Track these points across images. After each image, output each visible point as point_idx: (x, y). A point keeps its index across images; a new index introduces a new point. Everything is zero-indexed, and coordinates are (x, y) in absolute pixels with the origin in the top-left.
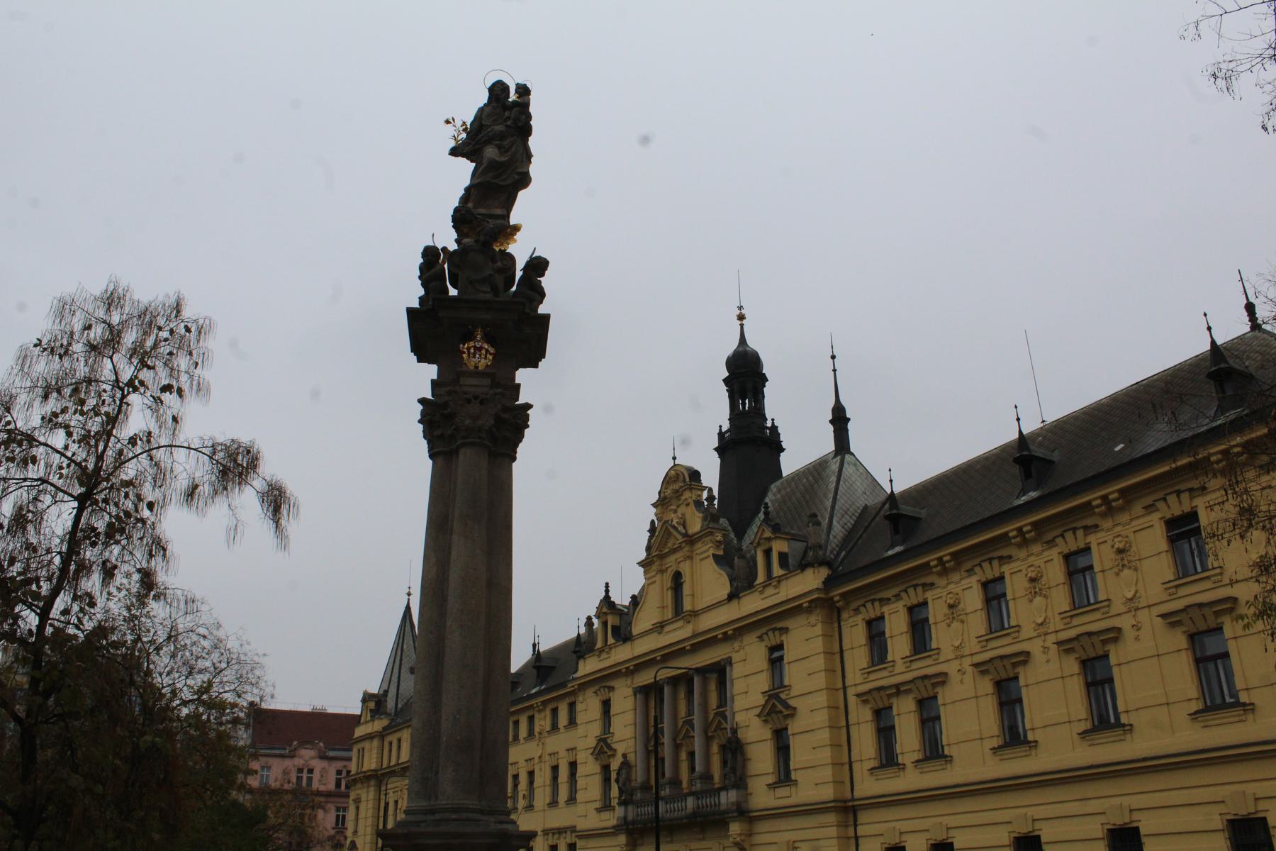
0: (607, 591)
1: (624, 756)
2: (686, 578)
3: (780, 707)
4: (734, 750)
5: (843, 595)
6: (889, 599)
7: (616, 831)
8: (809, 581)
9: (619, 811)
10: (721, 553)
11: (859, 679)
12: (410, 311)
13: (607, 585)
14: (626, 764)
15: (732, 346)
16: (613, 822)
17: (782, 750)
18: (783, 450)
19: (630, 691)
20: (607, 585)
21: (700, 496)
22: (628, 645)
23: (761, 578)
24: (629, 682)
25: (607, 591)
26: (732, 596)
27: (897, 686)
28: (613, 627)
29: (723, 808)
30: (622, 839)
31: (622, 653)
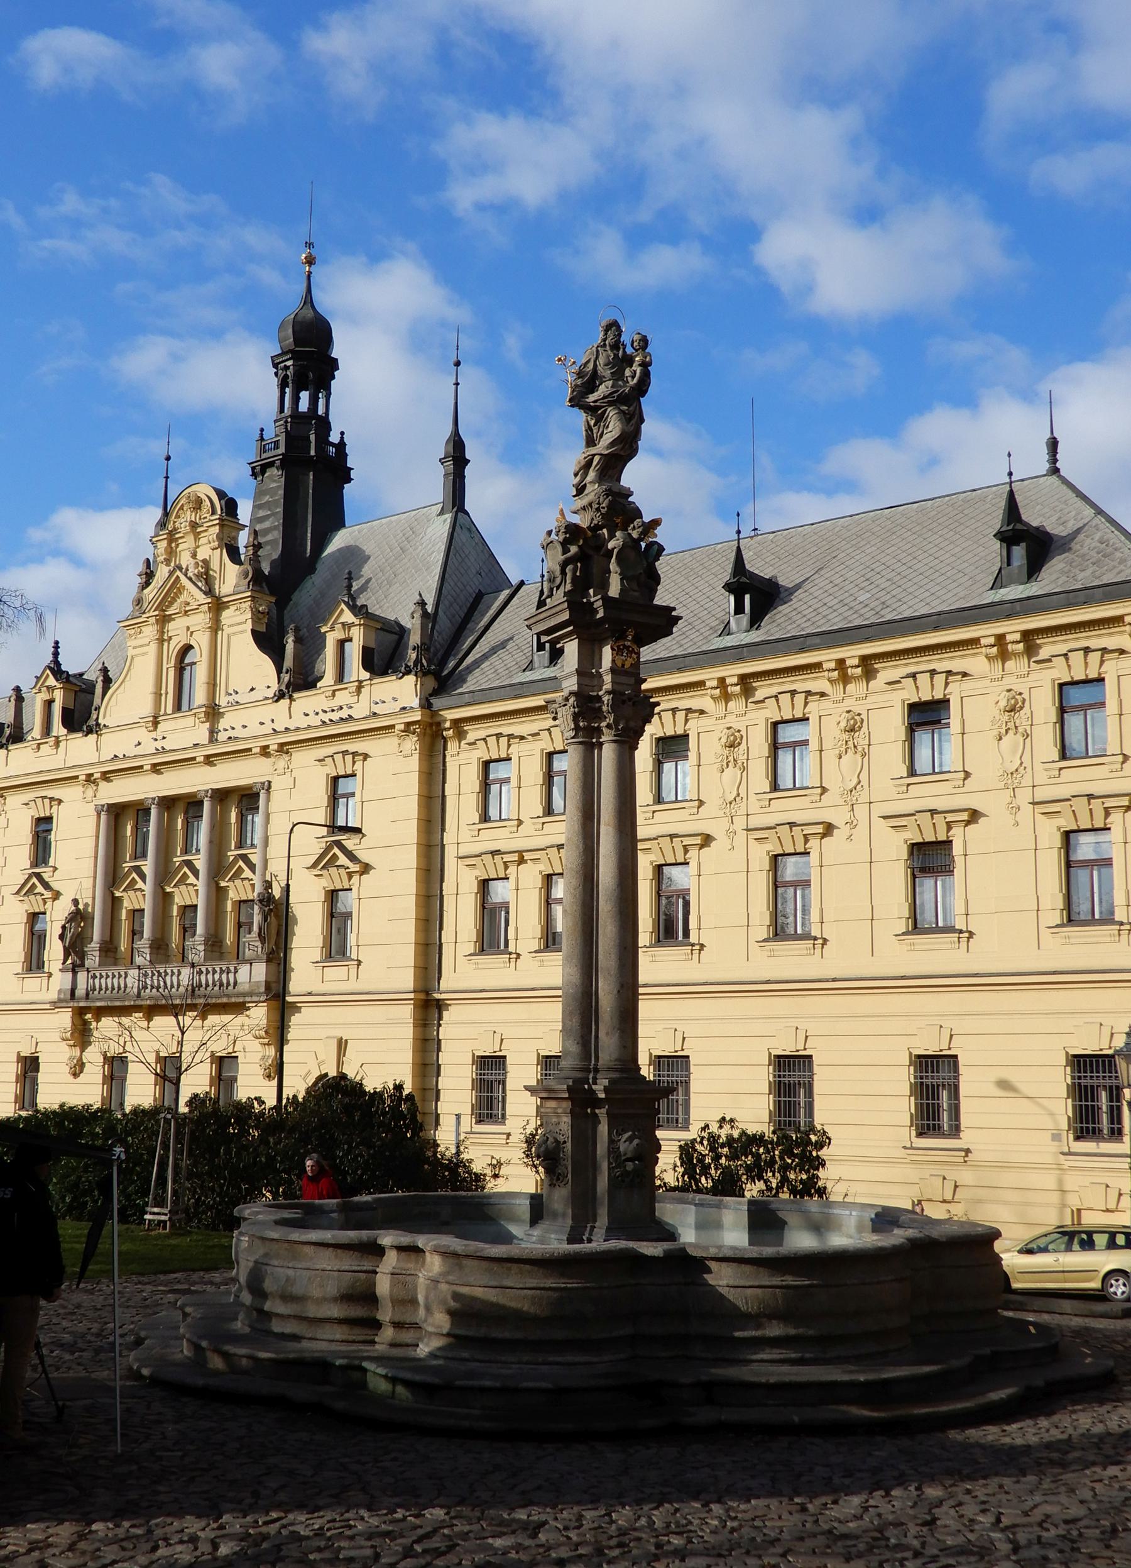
0: (56, 654)
1: (76, 902)
2: (200, 657)
3: (343, 860)
4: (277, 913)
5: (457, 723)
6: (522, 738)
7: (56, 1005)
8: (401, 692)
9: (60, 981)
10: (263, 629)
11: (466, 834)
12: (349, 480)
13: (57, 643)
14: (79, 916)
15: (290, 304)
16: (54, 996)
17: (337, 920)
18: (349, 480)
19: (91, 810)
20: (57, 643)
21: (236, 539)
22: (92, 737)
23: (328, 679)
24: (90, 792)
25: (56, 654)
26: (280, 696)
27: (520, 853)
28: (65, 710)
29: (240, 988)
30: (64, 1019)
31: (80, 750)
